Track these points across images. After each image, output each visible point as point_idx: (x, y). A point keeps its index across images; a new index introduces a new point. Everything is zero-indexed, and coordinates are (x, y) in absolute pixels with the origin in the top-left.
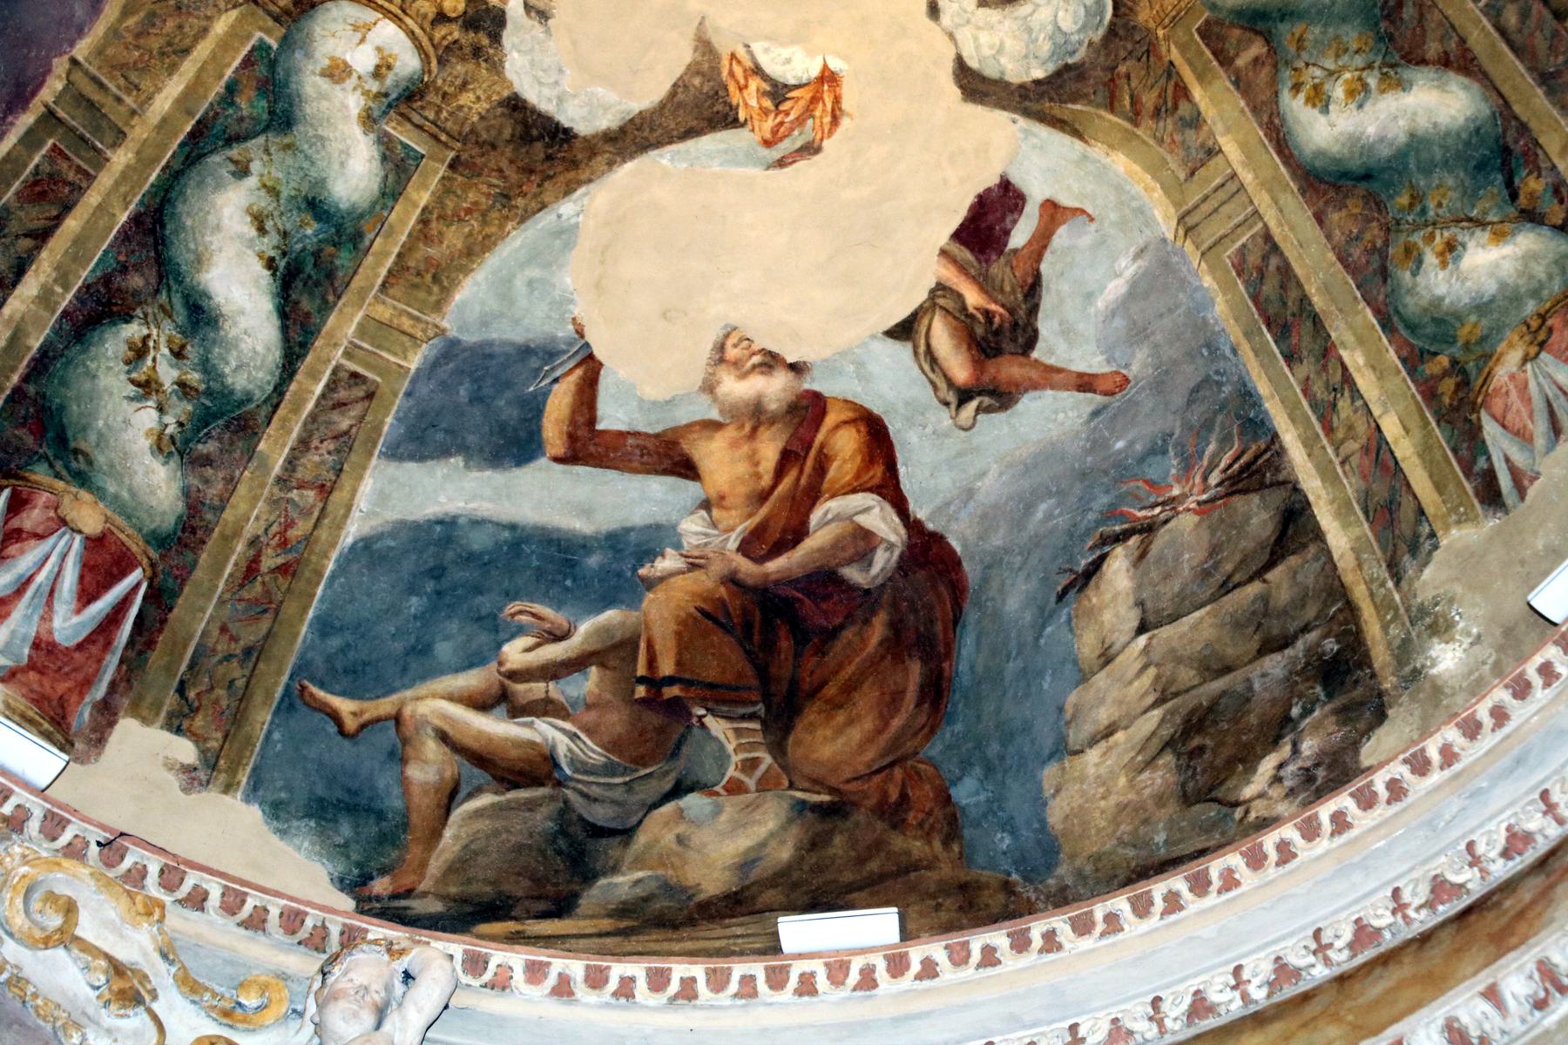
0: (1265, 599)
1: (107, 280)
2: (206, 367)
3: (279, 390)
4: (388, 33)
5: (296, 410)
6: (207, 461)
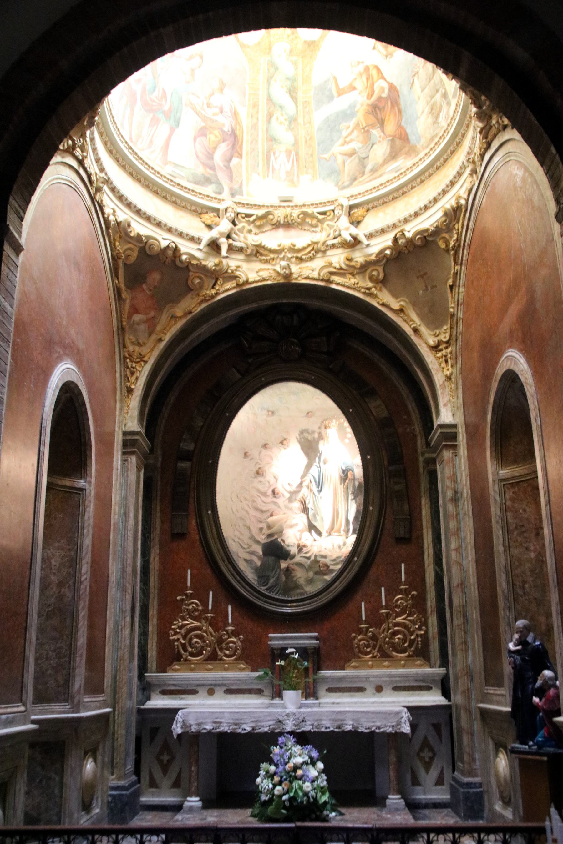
0: (434, 82)
1: (268, 112)
3: (297, 111)
6: (293, 128)
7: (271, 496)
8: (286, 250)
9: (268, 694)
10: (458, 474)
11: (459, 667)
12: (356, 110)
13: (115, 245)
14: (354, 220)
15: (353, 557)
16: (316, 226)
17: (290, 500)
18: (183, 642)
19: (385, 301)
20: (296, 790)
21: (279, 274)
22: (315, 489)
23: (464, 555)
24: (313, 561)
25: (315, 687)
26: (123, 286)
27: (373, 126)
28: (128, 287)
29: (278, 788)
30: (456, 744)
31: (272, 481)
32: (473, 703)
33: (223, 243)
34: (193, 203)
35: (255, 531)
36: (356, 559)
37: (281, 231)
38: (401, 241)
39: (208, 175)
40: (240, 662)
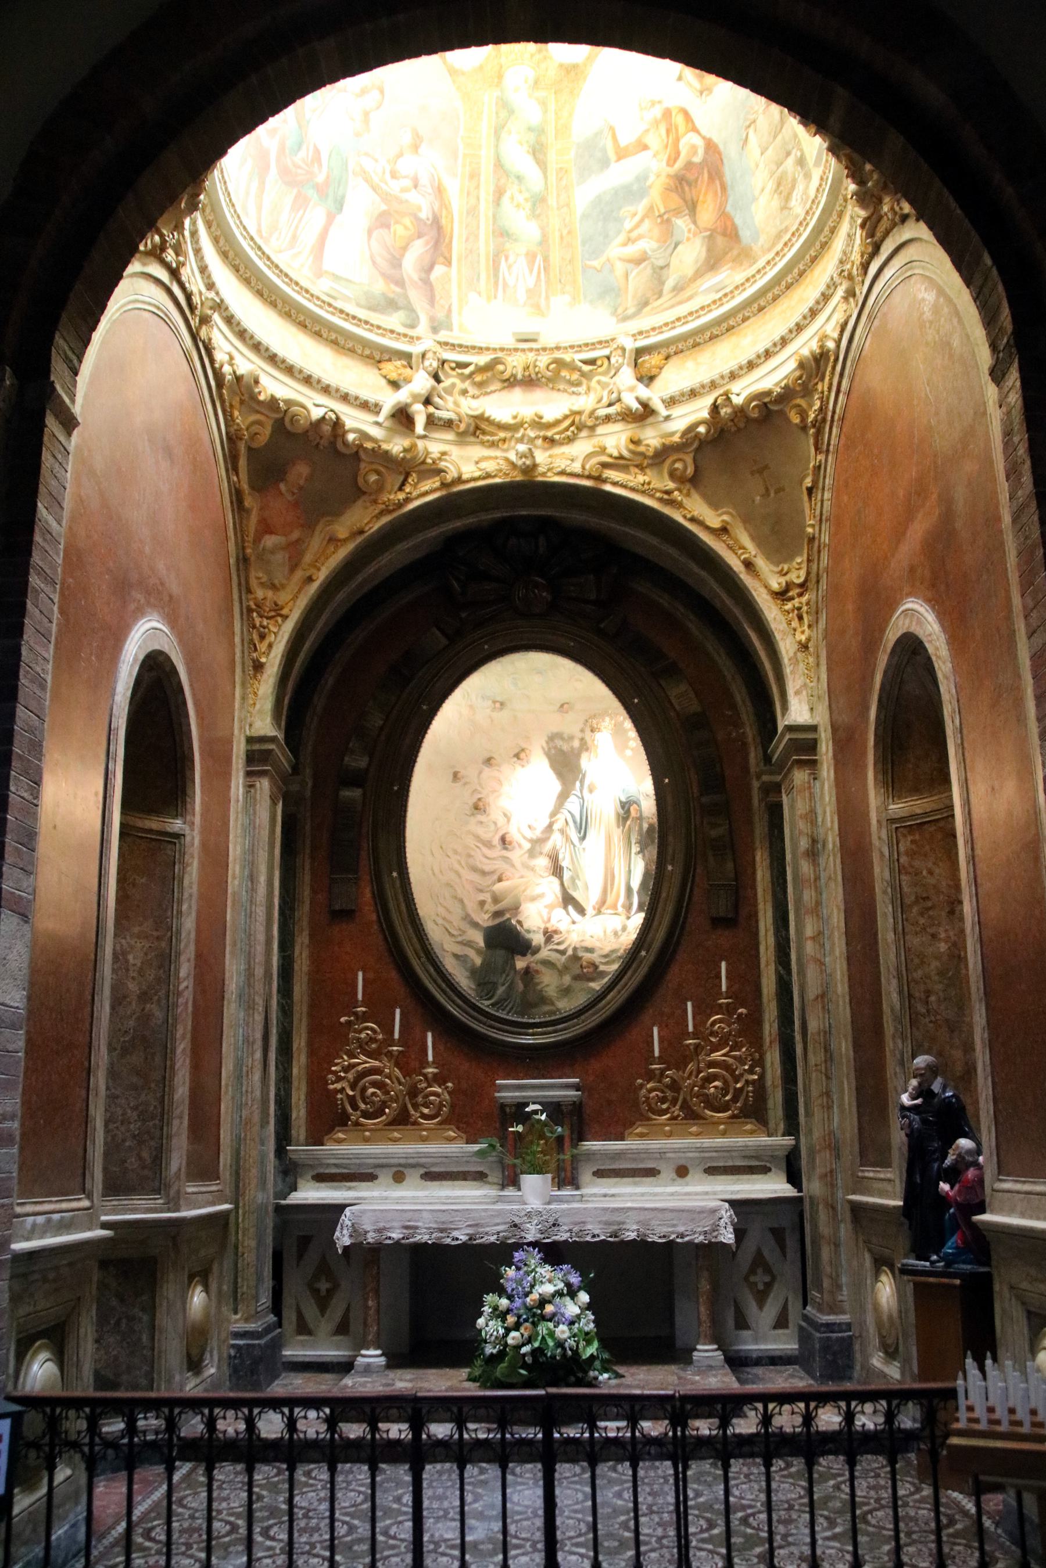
1: (497, 186)
3: (546, 183)
6: (539, 216)
7: (499, 847)
8: (526, 425)
9: (495, 1180)
10: (819, 811)
11: (816, 1134)
12: (648, 183)
13: (232, 416)
14: (644, 374)
15: (639, 952)
16: (578, 384)
17: (532, 853)
18: (351, 1093)
19: (695, 513)
20: (543, 1337)
21: (513, 465)
22: (574, 835)
23: (827, 947)
24: (570, 956)
25: (574, 1169)
26: (245, 487)
27: (677, 212)
28: (252, 487)
29: (513, 1334)
30: (809, 1263)
31: (501, 821)
32: (840, 1194)
33: (418, 412)
34: (366, 343)
35: (471, 907)
36: (643, 953)
37: (517, 393)
38: (725, 411)
39: (392, 296)
40: (447, 1127)
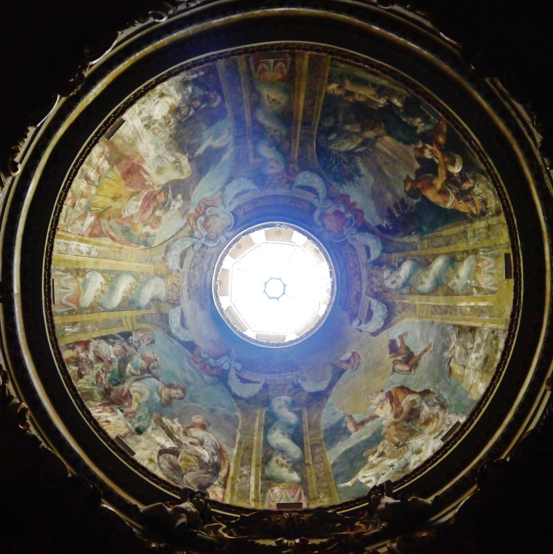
2: (289, 457)
4: (284, 398)
5: (308, 453)
12: (382, 434)
27: (407, 439)
